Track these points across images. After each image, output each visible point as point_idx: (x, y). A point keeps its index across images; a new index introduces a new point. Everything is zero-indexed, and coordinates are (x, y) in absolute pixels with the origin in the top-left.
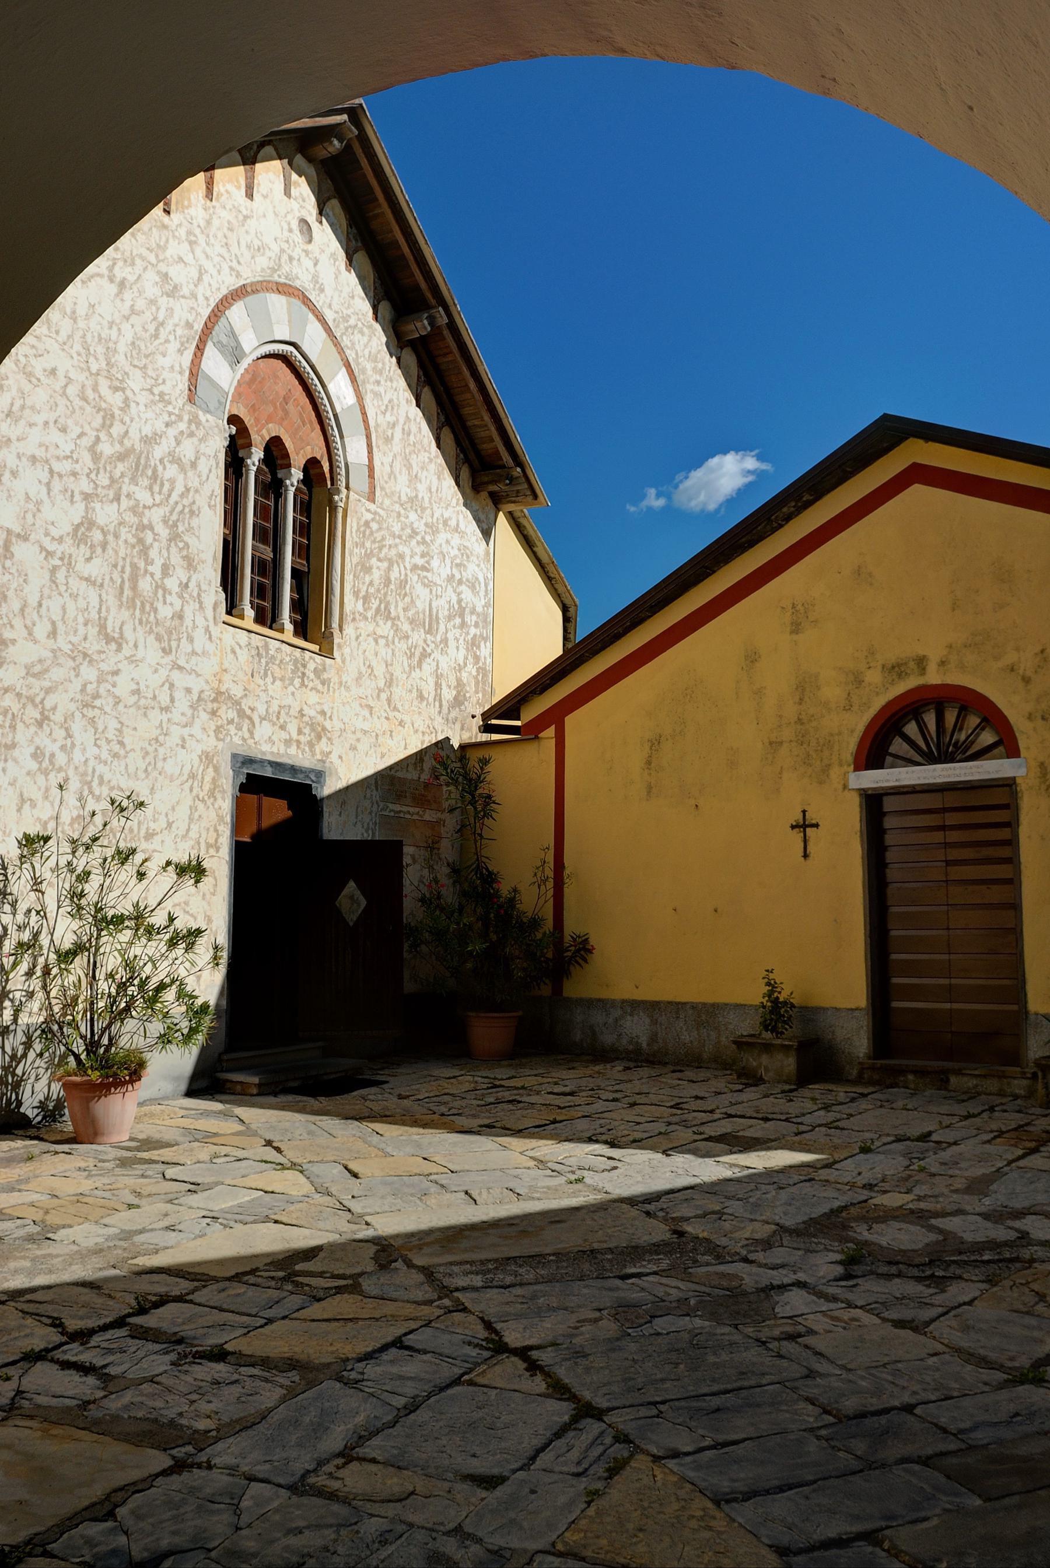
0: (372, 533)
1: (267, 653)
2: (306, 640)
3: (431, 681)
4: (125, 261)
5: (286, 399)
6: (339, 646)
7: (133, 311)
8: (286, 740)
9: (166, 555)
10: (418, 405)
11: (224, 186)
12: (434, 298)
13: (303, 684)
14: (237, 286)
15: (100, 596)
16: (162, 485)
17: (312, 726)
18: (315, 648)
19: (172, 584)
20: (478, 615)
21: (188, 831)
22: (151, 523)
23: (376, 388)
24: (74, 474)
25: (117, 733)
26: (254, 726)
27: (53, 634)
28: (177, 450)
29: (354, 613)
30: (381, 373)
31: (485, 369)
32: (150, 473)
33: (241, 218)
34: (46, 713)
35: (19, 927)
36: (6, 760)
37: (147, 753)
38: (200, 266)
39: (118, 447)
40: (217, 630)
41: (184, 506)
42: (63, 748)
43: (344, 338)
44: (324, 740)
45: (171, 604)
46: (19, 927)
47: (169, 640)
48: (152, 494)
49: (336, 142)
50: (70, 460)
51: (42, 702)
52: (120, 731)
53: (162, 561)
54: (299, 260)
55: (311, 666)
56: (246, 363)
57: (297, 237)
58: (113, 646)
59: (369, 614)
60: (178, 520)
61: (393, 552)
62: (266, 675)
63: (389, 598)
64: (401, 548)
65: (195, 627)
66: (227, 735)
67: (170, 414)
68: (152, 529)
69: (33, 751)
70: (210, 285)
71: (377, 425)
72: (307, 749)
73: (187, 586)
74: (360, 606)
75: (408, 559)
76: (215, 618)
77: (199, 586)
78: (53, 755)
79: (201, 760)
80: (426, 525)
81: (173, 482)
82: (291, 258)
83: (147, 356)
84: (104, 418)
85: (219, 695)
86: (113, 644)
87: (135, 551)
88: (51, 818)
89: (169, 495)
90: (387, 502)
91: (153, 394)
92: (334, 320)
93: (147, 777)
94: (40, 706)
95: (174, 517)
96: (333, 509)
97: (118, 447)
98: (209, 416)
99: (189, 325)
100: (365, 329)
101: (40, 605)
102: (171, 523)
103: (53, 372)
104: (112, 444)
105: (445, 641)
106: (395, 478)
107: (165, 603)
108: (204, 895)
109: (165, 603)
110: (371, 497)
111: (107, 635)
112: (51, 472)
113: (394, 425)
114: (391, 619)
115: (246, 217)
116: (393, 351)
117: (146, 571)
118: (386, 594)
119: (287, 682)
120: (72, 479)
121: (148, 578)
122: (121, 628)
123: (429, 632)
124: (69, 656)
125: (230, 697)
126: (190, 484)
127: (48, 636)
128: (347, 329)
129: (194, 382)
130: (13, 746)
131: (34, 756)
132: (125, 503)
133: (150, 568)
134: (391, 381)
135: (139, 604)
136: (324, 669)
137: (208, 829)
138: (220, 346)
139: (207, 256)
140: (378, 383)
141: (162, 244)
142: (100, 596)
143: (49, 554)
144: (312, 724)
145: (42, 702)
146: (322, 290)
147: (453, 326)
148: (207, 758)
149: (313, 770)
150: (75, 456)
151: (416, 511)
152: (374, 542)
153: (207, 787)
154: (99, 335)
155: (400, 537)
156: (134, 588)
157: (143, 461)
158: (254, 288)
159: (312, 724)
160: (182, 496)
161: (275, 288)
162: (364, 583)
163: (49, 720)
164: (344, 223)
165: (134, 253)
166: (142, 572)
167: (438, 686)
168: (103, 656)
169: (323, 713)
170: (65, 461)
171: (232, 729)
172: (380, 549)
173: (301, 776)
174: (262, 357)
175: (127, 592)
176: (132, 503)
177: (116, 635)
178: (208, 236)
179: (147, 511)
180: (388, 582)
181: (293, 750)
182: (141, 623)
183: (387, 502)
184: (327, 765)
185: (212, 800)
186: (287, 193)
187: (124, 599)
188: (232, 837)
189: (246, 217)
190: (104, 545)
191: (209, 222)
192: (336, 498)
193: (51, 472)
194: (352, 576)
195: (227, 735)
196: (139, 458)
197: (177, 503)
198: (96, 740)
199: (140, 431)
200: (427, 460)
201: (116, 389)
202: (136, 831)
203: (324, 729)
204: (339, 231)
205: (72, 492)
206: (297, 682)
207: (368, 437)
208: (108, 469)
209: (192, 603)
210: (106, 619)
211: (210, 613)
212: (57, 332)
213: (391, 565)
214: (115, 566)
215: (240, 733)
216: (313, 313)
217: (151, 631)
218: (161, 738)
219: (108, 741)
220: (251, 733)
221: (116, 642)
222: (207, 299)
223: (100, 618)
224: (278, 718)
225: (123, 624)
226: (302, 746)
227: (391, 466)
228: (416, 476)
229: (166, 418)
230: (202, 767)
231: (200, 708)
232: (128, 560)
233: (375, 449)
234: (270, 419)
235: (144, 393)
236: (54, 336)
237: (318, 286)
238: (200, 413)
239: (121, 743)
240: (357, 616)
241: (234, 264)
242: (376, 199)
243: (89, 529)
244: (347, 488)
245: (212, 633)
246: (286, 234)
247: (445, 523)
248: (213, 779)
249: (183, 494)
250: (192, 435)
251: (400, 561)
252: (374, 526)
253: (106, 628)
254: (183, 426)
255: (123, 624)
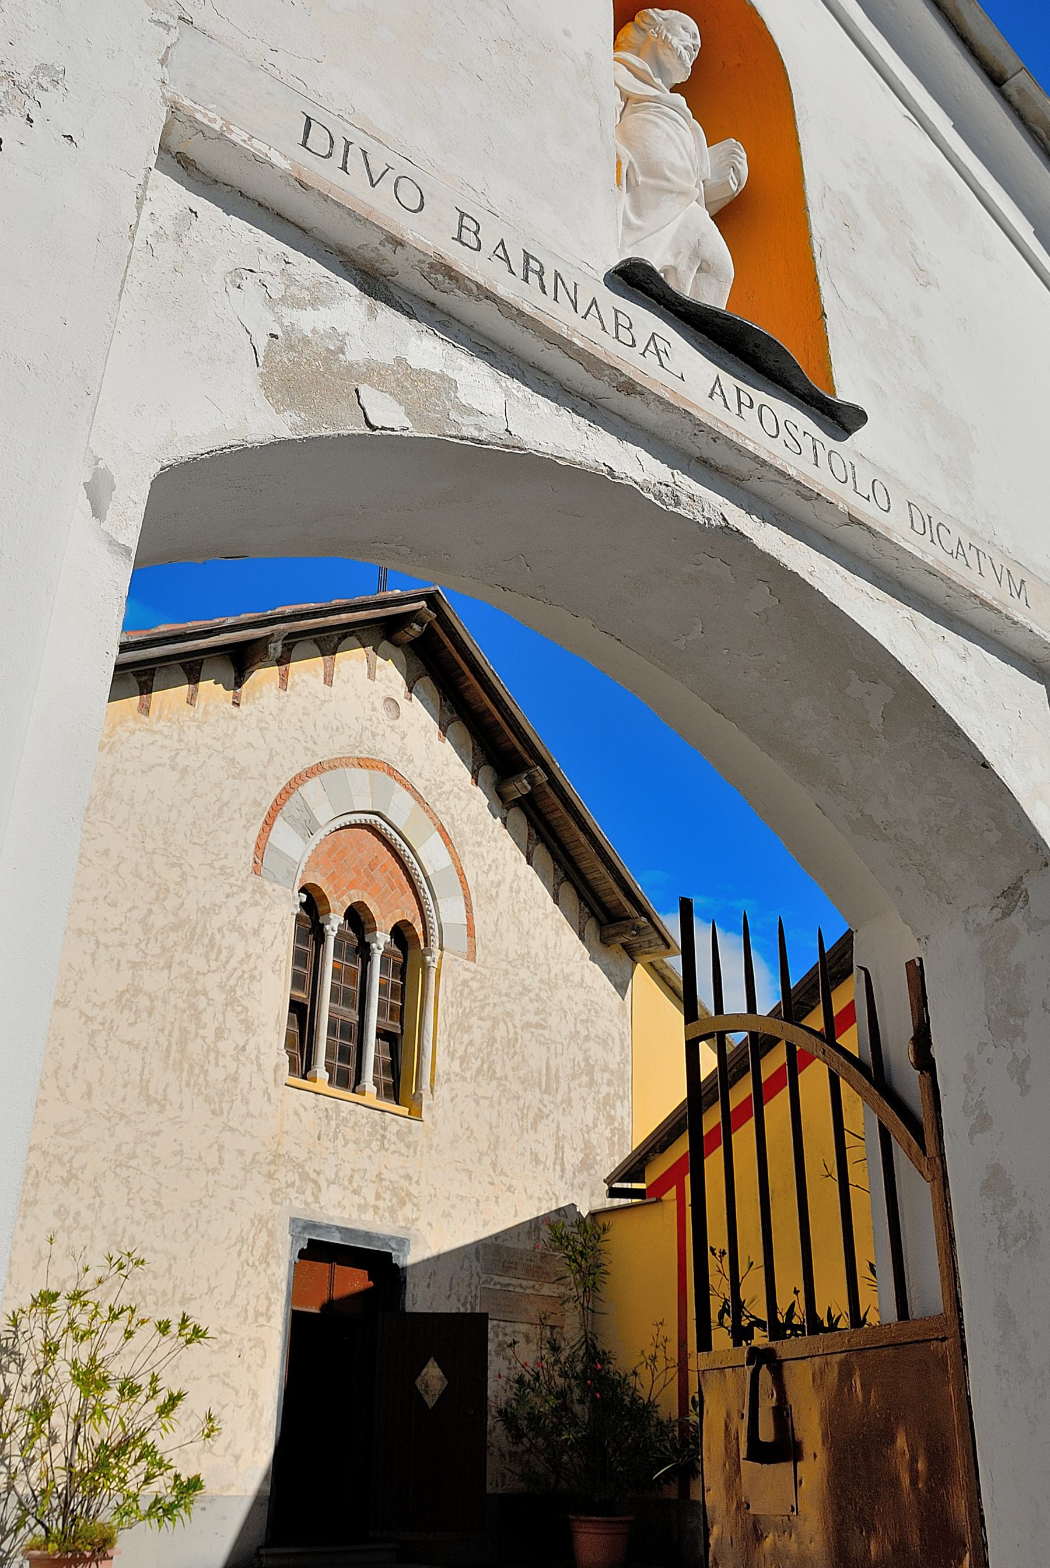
0: (472, 992)
1: (338, 1115)
2: (398, 1104)
3: (550, 1145)
4: (189, 750)
5: (372, 866)
6: (429, 1107)
7: (195, 794)
8: (359, 1205)
9: (221, 1019)
10: (529, 863)
11: (300, 676)
12: (531, 758)
13: (382, 1147)
14: (312, 764)
15: (143, 1059)
16: (220, 952)
17: (394, 1192)
18: (404, 1111)
19: (226, 1047)
20: (612, 1072)
21: (233, 1297)
22: (205, 989)
23: (477, 849)
24: (122, 945)
25: (154, 1194)
26: (320, 1190)
27: (89, 1094)
28: (238, 919)
29: (448, 1074)
30: (482, 834)
31: (593, 821)
32: (206, 941)
33: (318, 702)
34: (74, 1171)
35: (25, 1387)
36: (25, 1217)
37: (188, 1215)
38: (271, 750)
39: (171, 918)
40: (279, 1092)
41: (244, 972)
42: (90, 1206)
43: (437, 803)
44: (409, 1205)
45: (224, 1067)
46: (25, 1387)
47: (221, 1102)
48: (208, 961)
49: (416, 626)
50: (118, 932)
51: (70, 1161)
52: (158, 1192)
53: (217, 1025)
54: (383, 735)
55: (394, 1128)
56: (320, 835)
57: (382, 714)
58: (155, 1107)
59: (468, 1075)
60: (236, 985)
61: (499, 1010)
62: (336, 1137)
63: (493, 1057)
64: (508, 1006)
65: (251, 1088)
66: (285, 1198)
67: (231, 886)
68: (205, 994)
69: (56, 1208)
70: (282, 765)
71: (478, 885)
72: (387, 1215)
73: (244, 1048)
74: (456, 1066)
75: (517, 1017)
76: (275, 1080)
77: (258, 1048)
78: (78, 1213)
79: (253, 1224)
80: (541, 981)
81: (231, 949)
82: (374, 735)
83: (208, 834)
84: (158, 893)
85: (276, 1158)
86: (155, 1105)
87: (185, 1015)
88: (71, 1277)
89: (227, 962)
90: (491, 960)
91: (214, 868)
92: (425, 788)
93: (187, 1239)
94: (68, 1165)
95: (232, 982)
96: (426, 968)
97: (171, 918)
98: (275, 886)
99: (256, 803)
100: (462, 793)
101: (76, 1067)
102: (228, 988)
103: (106, 852)
104: (165, 916)
105: (569, 1101)
106: (501, 935)
107: (217, 1065)
108: (249, 1367)
109: (217, 1065)
110: (472, 956)
111: (148, 1096)
112: (97, 943)
113: (499, 884)
114: (496, 1079)
115: (323, 702)
116: (496, 812)
117: (197, 1035)
118: (489, 1054)
119: (362, 1145)
120: (119, 949)
121: (199, 1041)
122: (165, 1090)
123: (547, 1091)
124: (104, 1116)
125: (290, 1159)
126: (251, 951)
127: (82, 1097)
128: (440, 795)
129: (259, 854)
130: (35, 1203)
131: (57, 1213)
132: (176, 970)
133: (201, 1031)
134: (495, 840)
135: (186, 1066)
136: (410, 1132)
137: (258, 1297)
138: (292, 821)
139: (280, 740)
140: (479, 844)
141: (230, 732)
142: (143, 1059)
143: (89, 1019)
144: (394, 1189)
145: (70, 1161)
146: (410, 761)
147: (553, 782)
148: (261, 1222)
149: (393, 1238)
150: (124, 928)
151: (528, 967)
152: (475, 1000)
153: (258, 1252)
154: (158, 817)
155: (507, 995)
156: (182, 1051)
157: (199, 931)
158: (332, 765)
159: (394, 1189)
160: (242, 962)
161: (356, 763)
162: (461, 1043)
163: (77, 1179)
164: (437, 697)
165: (200, 742)
166: (192, 1035)
167: (559, 1148)
168: (142, 1117)
169: (408, 1177)
170: (112, 933)
171: (292, 1192)
172: (483, 1008)
173: (379, 1243)
174: (341, 828)
175: (174, 1055)
176: (185, 970)
177: (159, 1097)
178: (281, 722)
179: (200, 977)
180: (492, 1041)
181: (368, 1216)
182: (188, 1084)
183: (491, 960)
184: (413, 1232)
185: (264, 1265)
186: (371, 675)
187: (171, 1062)
188: (287, 1306)
189: (323, 702)
190: (150, 1012)
191: (282, 710)
192: (428, 958)
193: (97, 943)
194: (446, 1036)
195: (285, 1198)
196: (195, 927)
197: (235, 969)
198: (129, 1200)
199: (197, 903)
200: (541, 916)
201: (174, 865)
202: (170, 1295)
203: (409, 1194)
204: (431, 705)
205: (119, 961)
206: (375, 1145)
207: (467, 897)
208: (160, 939)
209: (249, 1065)
210: (148, 1081)
211: (269, 1075)
212: (112, 818)
213: (496, 1022)
214: (162, 1030)
215: (302, 1197)
216: (400, 782)
217: (200, 1093)
218: (206, 1200)
219: (143, 1202)
220: (316, 1198)
221: (159, 1104)
222: (278, 778)
223: (141, 1080)
224: (351, 1183)
225: (167, 1085)
226: (381, 1212)
227: (496, 925)
228: (527, 933)
229: (228, 890)
230: (253, 1231)
231: (254, 1171)
232: (177, 1024)
233: (475, 908)
234: (352, 885)
235: (202, 867)
236: (110, 821)
237: (405, 757)
238: (266, 883)
239: (158, 1204)
240: (453, 1077)
241: (310, 745)
242: (464, 674)
243: (134, 995)
244: (441, 948)
245: (272, 1095)
246: (369, 713)
247: (566, 978)
248: (267, 1243)
249: (243, 960)
250: (256, 904)
251: (508, 1020)
252: (475, 985)
253: (148, 1090)
254: (245, 896)
255: (167, 1085)
